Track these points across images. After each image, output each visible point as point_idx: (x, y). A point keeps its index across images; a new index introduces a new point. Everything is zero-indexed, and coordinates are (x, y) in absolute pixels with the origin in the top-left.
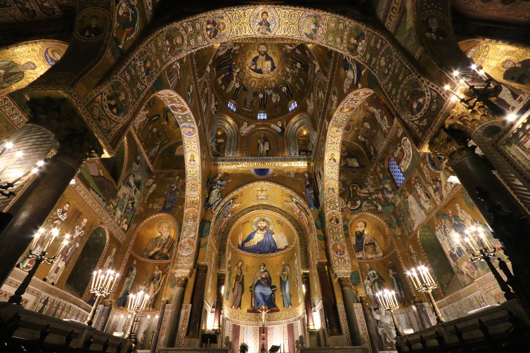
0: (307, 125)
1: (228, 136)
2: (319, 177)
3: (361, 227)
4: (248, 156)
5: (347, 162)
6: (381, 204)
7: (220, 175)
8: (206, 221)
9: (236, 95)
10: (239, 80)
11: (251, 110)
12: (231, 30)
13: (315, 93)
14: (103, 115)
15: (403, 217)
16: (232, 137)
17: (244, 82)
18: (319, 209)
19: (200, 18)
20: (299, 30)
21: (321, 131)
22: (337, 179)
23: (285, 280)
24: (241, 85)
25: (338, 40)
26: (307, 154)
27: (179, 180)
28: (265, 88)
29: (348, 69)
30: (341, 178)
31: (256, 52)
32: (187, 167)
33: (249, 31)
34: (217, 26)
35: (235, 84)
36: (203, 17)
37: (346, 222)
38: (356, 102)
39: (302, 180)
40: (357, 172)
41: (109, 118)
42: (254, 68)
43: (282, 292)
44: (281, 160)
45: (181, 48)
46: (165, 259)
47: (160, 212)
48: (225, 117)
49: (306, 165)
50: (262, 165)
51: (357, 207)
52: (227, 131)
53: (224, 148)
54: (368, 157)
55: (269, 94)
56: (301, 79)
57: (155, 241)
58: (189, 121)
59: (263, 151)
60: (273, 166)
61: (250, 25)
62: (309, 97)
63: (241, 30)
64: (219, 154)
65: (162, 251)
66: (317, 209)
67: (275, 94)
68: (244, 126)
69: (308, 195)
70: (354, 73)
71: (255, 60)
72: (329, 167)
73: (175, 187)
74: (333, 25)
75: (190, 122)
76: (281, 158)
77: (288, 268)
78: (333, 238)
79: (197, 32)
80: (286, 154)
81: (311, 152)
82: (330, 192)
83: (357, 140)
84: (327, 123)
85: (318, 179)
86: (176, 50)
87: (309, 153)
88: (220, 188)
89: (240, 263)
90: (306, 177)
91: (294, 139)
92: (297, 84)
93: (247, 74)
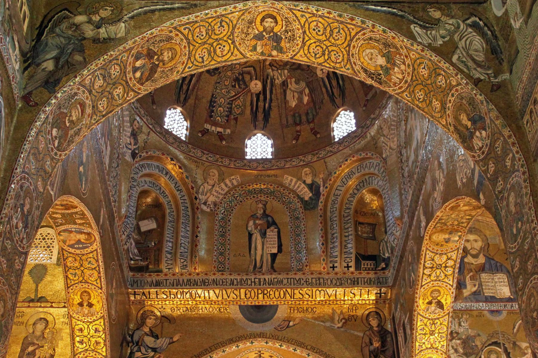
1: (168, 211)
2: (403, 334)
16: (178, 216)
20: (349, 60)
26: (377, 266)
33: (232, 53)
44: (309, 284)
49: (373, 297)
50: (261, 296)
58: (79, 221)
59: (262, 256)
63: (212, 54)
64: (147, 266)
68: (211, 182)
72: (426, 320)
74: (425, 72)
76: (310, 277)
81: (387, 261)
84: (423, 218)
85: (401, 339)
87: (383, 265)
90: (371, 327)
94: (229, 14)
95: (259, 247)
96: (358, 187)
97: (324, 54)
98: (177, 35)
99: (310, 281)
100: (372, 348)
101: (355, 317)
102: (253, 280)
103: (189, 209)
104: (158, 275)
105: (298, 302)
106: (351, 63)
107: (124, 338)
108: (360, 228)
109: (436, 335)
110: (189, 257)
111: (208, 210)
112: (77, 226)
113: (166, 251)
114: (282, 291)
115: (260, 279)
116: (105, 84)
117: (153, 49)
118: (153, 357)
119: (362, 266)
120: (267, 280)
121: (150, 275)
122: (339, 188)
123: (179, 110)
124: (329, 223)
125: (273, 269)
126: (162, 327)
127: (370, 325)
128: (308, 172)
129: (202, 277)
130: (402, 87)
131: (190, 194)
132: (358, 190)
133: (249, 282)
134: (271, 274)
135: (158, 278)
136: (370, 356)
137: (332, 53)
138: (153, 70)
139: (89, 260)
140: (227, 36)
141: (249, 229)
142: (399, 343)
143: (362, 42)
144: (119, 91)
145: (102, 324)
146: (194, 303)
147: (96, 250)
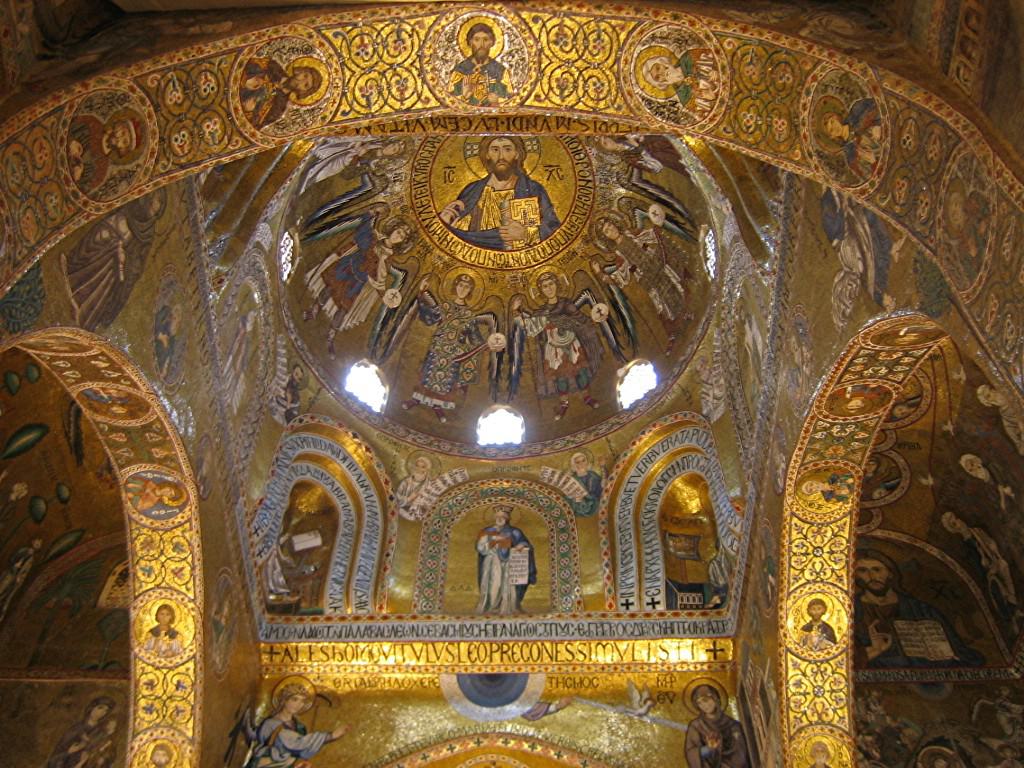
0: (702, 468)
1: (342, 518)
5: (897, 642)
7: (295, 705)
9: (385, 338)
10: (401, 275)
11: (451, 405)
12: (344, 94)
17: (423, 284)
19: (216, 55)
20: (619, 89)
22: (846, 725)
24: (413, 298)
25: (781, 125)
27: (102, 723)
28: (516, 305)
29: (839, 234)
30: (871, 718)
31: (475, 163)
32: (140, 664)
33: (419, 97)
34: (284, 80)
35: (381, 294)
36: (231, 51)
38: (890, 371)
40: (949, 687)
42: (466, 229)
44: (584, 634)
48: (332, 434)
49: (703, 656)
54: (992, 611)
55: (532, 333)
56: (668, 270)
58: (159, 453)
59: (500, 590)
60: (547, 660)
61: (421, 72)
63: (386, 92)
64: (298, 604)
68: (419, 477)
70: (863, 253)
71: (471, 194)
72: (803, 665)
74: (752, 72)
75: (161, 461)
76: (585, 622)
79: (201, 104)
81: (723, 591)
83: (936, 535)
84: (780, 459)
85: (756, 723)
86: (108, 175)
90: (702, 714)
91: (648, 533)
92: (654, 293)
93: (438, 252)
94: (411, 17)
96: (666, 476)
97: (576, 88)
98: (322, 45)
99: (586, 628)
100: (705, 751)
101: (671, 695)
102: (483, 627)
104: (314, 620)
105: (564, 668)
106: (623, 95)
108: (671, 543)
109: (827, 695)
110: (372, 589)
111: (412, 518)
114: (535, 647)
115: (495, 626)
116: (187, 104)
117: (279, 62)
118: (293, 765)
119: (679, 602)
120: (508, 626)
121: (301, 620)
122: (632, 480)
123: (377, 409)
124: (618, 535)
125: (519, 610)
126: (316, 713)
127: (699, 709)
129: (394, 622)
130: (715, 116)
131: (381, 493)
132: (665, 481)
133: (476, 631)
134: (516, 617)
135: (315, 625)
136: (702, 765)
137: (590, 82)
138: (279, 103)
139: (175, 541)
140: (410, 61)
141: (480, 548)
142: (756, 733)
143: (640, 48)
144: (213, 127)
145: (191, 672)
146: (377, 669)
147: (189, 520)
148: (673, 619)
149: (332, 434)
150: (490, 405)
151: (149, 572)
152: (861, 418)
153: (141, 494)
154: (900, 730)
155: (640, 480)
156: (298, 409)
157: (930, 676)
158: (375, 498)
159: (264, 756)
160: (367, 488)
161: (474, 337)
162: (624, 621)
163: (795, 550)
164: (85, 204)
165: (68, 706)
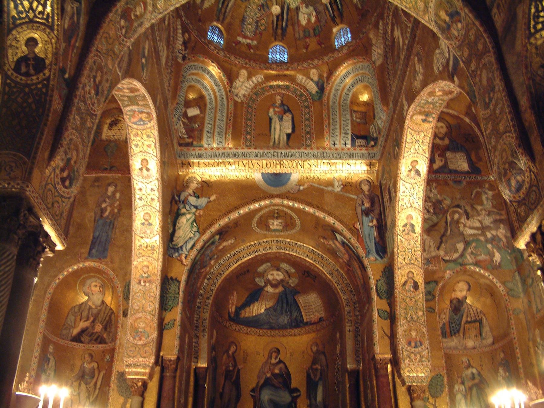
1: (208, 101)
2: (388, 197)
3: (461, 291)
4: (249, 147)
6: (499, 249)
7: (194, 186)
8: (172, 278)
13: (388, 24)
14: (55, 196)
15: (533, 279)
18: (385, 260)
21: (394, 112)
22: (421, 208)
23: (317, 379)
26: (367, 143)
27: (114, 194)
30: (432, 195)
32: (135, 182)
37: (433, 285)
39: (355, 197)
40: (465, 183)
41: (62, 196)
43: (310, 400)
45: (141, 21)
46: (100, 343)
47: (86, 259)
50: (278, 166)
51: (456, 255)
52: (207, 90)
53: (201, 130)
57: (79, 309)
58: (141, 103)
59: (279, 136)
60: (299, 167)
62: (376, 26)
65: (93, 327)
66: (382, 258)
67: (307, 7)
69: (366, 230)
73: (109, 209)
75: (142, 105)
76: (316, 151)
77: (322, 357)
78: (406, 318)
80: (327, 143)
81: (376, 140)
82: (406, 231)
85: (385, 200)
86: (134, 27)
88: (194, 213)
89: (233, 349)
90: (363, 191)
91: (344, 110)
95: (278, 127)
96: (353, 84)
100: (363, 208)
103: (225, 100)
104: (199, 149)
107: (173, 198)
108: (354, 115)
112: (140, 107)
113: (207, 131)
115: (278, 153)
121: (194, 149)
124: (331, 110)
125: (288, 146)
128: (315, 73)
133: (270, 155)
139: (147, 134)
141: (270, 115)
148: (354, 151)
149: (203, 62)
150: (272, 42)
151: (137, 146)
152: (441, 97)
153: (133, 116)
154: (442, 201)
155: (342, 85)
156: (187, 54)
157: (458, 178)
158: (223, 91)
159: (183, 208)
160: (217, 86)
161: (265, 7)
162: (333, 151)
163: (408, 140)
164: (126, 42)
165: (98, 186)
